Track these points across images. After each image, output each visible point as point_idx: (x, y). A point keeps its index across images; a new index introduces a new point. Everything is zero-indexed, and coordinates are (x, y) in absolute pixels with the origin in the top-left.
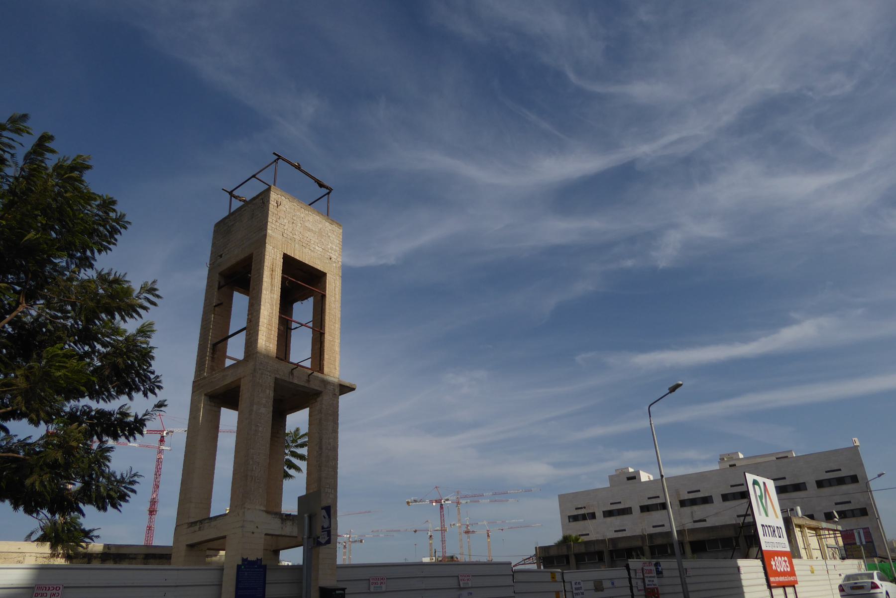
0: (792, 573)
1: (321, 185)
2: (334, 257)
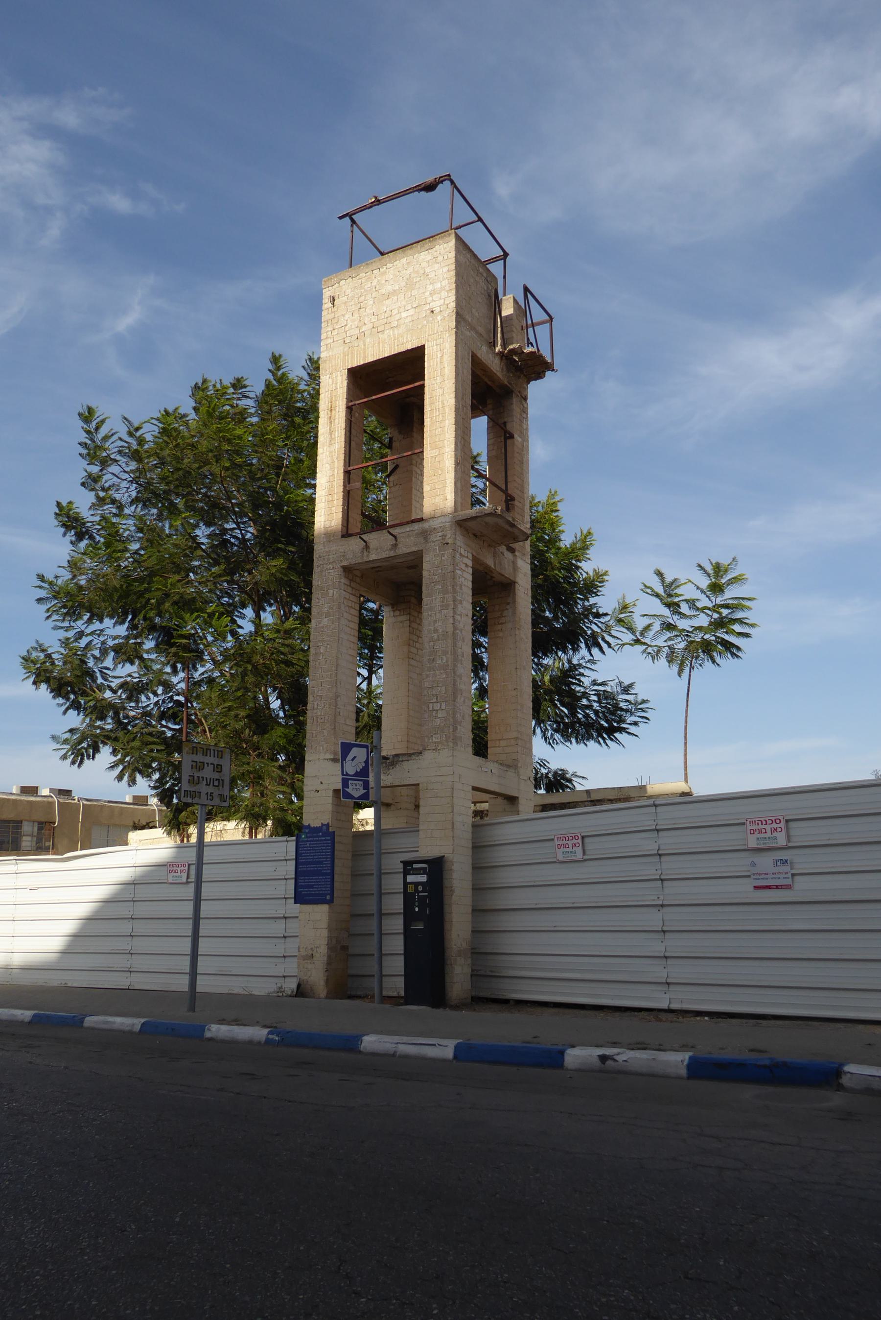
1: (430, 187)
2: (436, 305)
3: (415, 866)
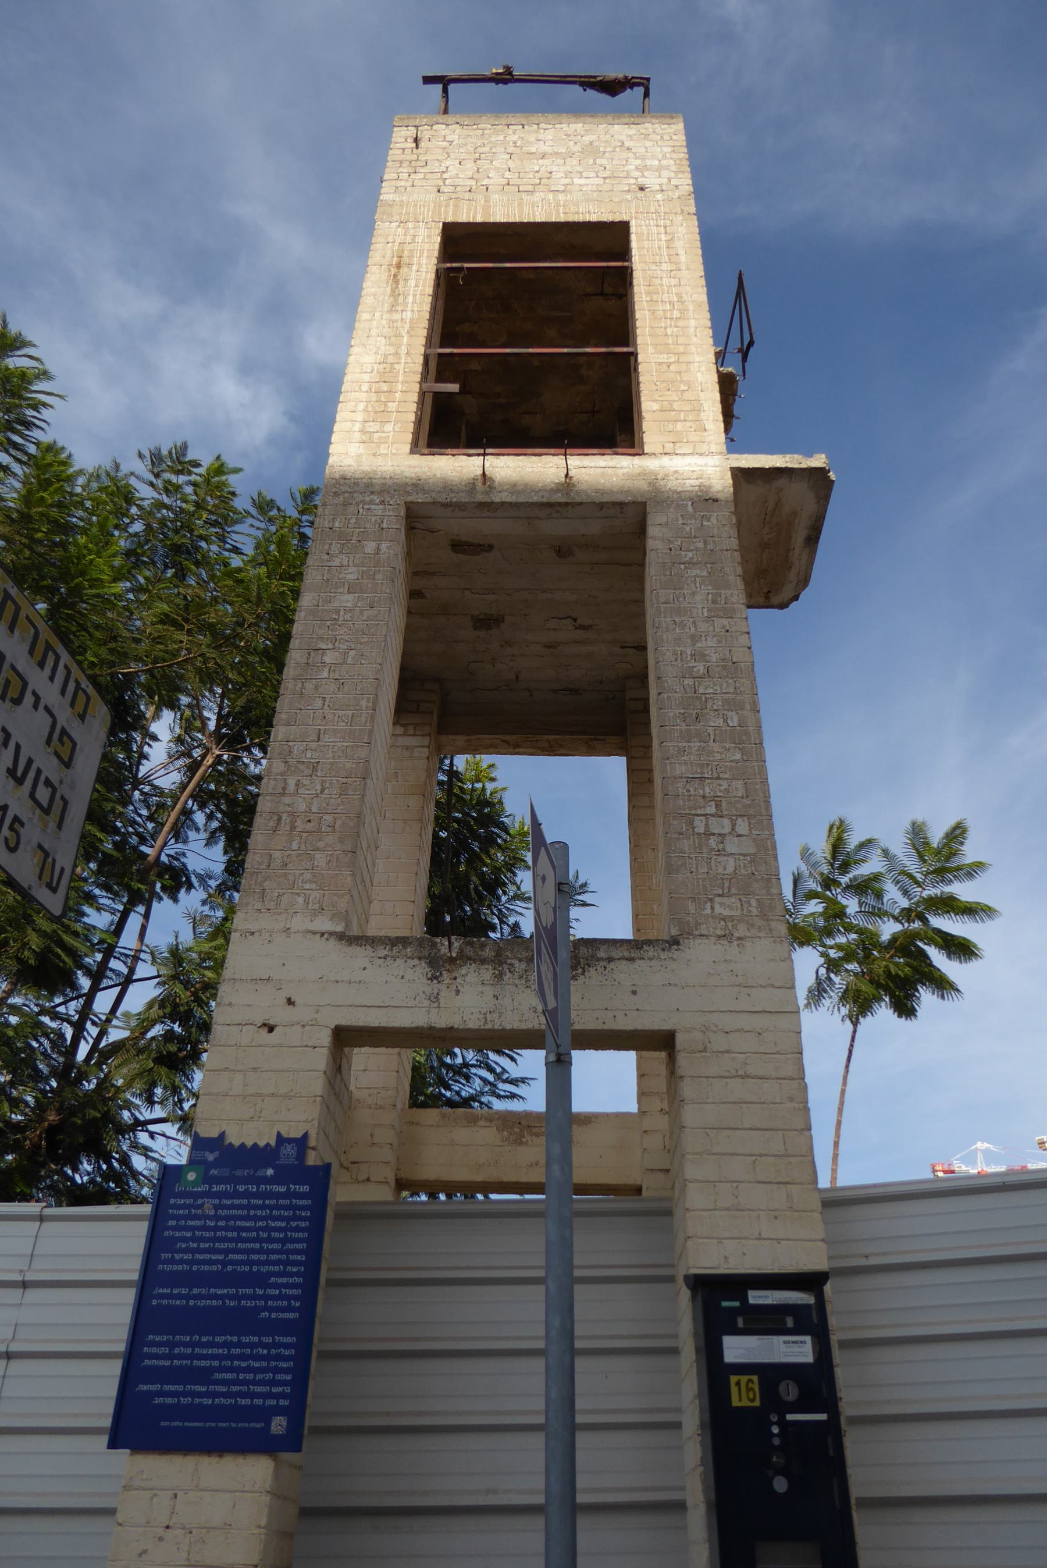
2: (651, 181)
3: (757, 1297)
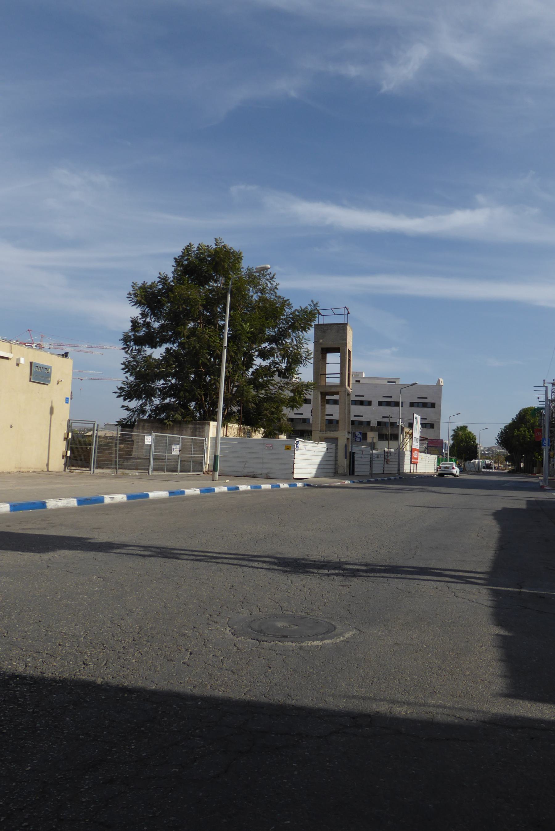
0: (417, 459)
